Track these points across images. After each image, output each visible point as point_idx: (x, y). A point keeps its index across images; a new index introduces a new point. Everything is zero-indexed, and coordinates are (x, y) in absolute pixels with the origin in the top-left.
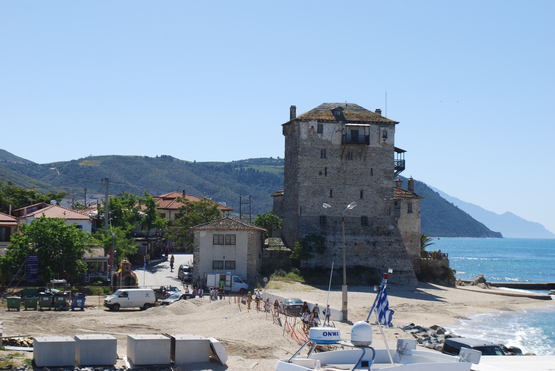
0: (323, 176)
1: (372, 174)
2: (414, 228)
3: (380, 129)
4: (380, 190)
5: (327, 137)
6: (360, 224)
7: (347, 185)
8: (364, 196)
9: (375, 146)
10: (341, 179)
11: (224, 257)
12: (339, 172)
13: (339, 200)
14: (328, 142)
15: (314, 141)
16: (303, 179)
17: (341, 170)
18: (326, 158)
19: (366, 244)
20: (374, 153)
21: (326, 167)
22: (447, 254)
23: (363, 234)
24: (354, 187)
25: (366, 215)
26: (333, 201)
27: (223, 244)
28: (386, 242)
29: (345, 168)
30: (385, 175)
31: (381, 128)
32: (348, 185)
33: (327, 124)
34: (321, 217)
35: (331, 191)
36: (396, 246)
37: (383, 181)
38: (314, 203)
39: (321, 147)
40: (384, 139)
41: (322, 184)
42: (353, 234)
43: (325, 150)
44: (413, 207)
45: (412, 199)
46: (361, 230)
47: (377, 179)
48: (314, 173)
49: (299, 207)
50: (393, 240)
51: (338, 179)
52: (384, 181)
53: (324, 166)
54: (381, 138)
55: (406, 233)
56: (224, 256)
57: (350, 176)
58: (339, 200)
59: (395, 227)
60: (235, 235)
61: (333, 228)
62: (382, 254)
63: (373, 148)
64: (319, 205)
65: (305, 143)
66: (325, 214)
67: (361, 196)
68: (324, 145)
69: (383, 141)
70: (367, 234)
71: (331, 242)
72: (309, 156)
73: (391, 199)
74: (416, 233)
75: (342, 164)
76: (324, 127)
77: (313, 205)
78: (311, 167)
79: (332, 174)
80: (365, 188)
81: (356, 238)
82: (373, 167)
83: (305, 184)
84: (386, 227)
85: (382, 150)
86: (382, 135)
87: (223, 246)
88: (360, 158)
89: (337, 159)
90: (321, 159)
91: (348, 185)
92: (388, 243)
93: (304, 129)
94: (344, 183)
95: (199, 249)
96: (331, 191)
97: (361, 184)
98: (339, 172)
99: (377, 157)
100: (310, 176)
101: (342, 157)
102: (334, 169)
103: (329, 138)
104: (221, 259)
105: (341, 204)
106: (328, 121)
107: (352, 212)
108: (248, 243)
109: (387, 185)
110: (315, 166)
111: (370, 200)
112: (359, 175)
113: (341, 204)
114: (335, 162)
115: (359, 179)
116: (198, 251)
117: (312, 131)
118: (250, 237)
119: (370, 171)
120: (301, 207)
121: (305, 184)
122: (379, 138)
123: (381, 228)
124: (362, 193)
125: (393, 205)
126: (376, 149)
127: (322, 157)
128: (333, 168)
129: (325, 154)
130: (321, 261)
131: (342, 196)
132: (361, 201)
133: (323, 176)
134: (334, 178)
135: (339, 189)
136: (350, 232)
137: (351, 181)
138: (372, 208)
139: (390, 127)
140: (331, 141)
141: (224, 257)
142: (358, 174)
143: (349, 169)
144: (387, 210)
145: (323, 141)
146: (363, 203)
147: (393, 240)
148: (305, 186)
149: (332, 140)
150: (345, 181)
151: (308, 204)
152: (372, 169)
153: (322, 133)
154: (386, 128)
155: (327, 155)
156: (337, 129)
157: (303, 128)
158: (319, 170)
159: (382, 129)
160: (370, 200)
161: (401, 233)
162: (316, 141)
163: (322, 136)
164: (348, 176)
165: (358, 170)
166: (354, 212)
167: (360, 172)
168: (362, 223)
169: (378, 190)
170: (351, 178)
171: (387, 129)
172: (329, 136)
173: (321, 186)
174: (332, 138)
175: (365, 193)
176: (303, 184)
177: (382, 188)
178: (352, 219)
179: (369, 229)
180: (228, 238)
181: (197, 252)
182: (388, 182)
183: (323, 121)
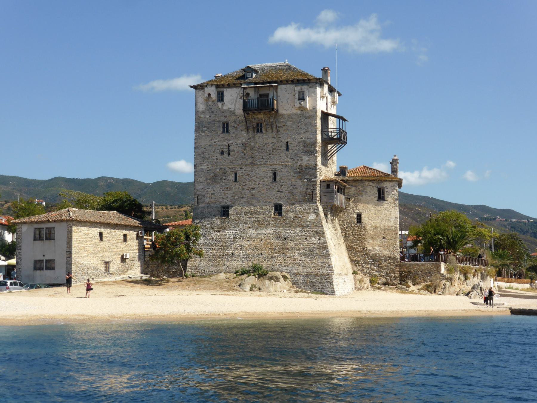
0: (226, 155)
1: (287, 148)
4: (298, 169)
5: (230, 106)
7: (255, 164)
9: (291, 112)
10: (248, 157)
11: (44, 256)
12: (245, 149)
13: (246, 185)
14: (231, 112)
15: (213, 112)
16: (201, 161)
17: (248, 147)
18: (229, 133)
20: (290, 122)
21: (229, 144)
24: (264, 167)
26: (237, 186)
27: (43, 240)
30: (305, 149)
31: (296, 88)
32: (257, 164)
33: (229, 90)
35: (236, 174)
36: (315, 240)
38: (214, 190)
39: (223, 119)
41: (224, 166)
44: (385, 193)
45: (385, 183)
47: (295, 155)
48: (214, 152)
51: (243, 158)
53: (226, 143)
55: (376, 227)
56: (107, 259)
57: (259, 153)
58: (246, 185)
59: (317, 216)
60: (54, 228)
62: (294, 251)
64: (221, 193)
65: (202, 116)
66: (229, 204)
67: (274, 179)
68: (225, 117)
69: (299, 105)
74: (392, 227)
76: (226, 93)
77: (213, 192)
78: (210, 145)
79: (236, 152)
83: (203, 167)
85: (301, 117)
87: (43, 241)
89: (243, 132)
90: (223, 135)
91: (257, 164)
92: (304, 238)
94: (252, 163)
95: (21, 246)
96: (236, 174)
99: (294, 126)
100: (209, 157)
101: (247, 129)
102: (239, 145)
103: (232, 107)
104: (41, 258)
105: (248, 189)
106: (229, 86)
107: (263, 200)
108: (67, 237)
110: (215, 144)
111: (286, 183)
112: (271, 152)
113: (248, 189)
114: (240, 137)
115: (270, 157)
116: (20, 249)
120: (198, 197)
121: (203, 167)
123: (298, 218)
124: (274, 174)
126: (293, 117)
127: (223, 132)
128: (238, 145)
130: (213, 262)
132: (274, 184)
133: (226, 155)
134: (239, 157)
135: (245, 171)
136: (256, 224)
137: (261, 160)
139: (311, 85)
140: (234, 110)
141: (44, 256)
142: (269, 151)
143: (257, 145)
144: (309, 195)
146: (276, 187)
149: (236, 109)
150: (253, 160)
151: (207, 192)
152: (287, 143)
154: (303, 87)
155: (229, 128)
157: (200, 97)
159: (298, 88)
160: (286, 183)
161: (367, 228)
162: (216, 112)
163: (222, 105)
164: (257, 154)
165: (269, 145)
167: (272, 147)
169: (296, 169)
171: (305, 88)
172: (232, 104)
173: (222, 168)
175: (278, 173)
176: (200, 167)
177: (301, 166)
180: (48, 232)
181: (20, 250)
182: (308, 158)
183: (223, 86)
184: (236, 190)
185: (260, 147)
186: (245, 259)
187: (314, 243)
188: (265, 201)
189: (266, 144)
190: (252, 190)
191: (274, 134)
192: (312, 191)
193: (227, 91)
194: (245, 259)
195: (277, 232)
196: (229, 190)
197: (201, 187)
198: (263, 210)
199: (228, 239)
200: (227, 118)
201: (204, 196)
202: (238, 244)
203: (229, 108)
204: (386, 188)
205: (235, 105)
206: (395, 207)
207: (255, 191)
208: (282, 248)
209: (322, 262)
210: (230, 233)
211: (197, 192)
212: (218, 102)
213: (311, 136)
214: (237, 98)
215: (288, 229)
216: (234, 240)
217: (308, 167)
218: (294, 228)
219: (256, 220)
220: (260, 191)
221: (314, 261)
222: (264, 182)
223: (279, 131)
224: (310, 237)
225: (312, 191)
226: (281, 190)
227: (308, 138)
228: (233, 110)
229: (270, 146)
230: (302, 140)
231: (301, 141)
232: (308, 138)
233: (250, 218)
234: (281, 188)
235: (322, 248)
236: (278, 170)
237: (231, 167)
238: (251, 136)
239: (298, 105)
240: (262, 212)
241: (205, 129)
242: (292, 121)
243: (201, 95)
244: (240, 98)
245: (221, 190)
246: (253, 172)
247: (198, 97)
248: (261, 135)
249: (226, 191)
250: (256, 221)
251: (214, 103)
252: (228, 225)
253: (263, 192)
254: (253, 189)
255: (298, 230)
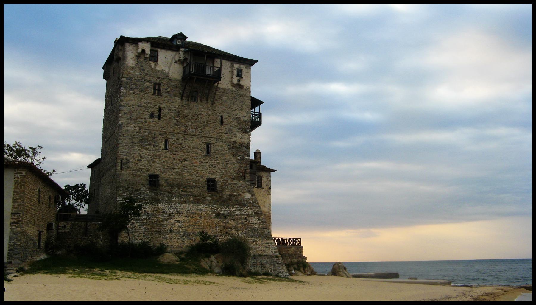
0: (156, 119)
1: (222, 122)
2: (265, 206)
3: (233, 66)
5: (163, 68)
6: (206, 188)
8: (212, 150)
12: (178, 116)
14: (164, 74)
15: (144, 70)
18: (161, 96)
19: (215, 218)
22: (301, 239)
23: (210, 203)
24: (198, 138)
25: (213, 177)
26: (168, 155)
28: (241, 214)
29: (186, 111)
32: (190, 135)
33: (163, 51)
34: (150, 176)
35: (166, 141)
36: (255, 220)
37: (236, 134)
38: (141, 157)
39: (155, 80)
40: (238, 78)
42: (197, 201)
43: (159, 85)
44: (262, 181)
45: (262, 172)
46: (208, 198)
49: (119, 161)
50: (250, 213)
52: (237, 134)
53: (158, 106)
54: (235, 77)
57: (192, 123)
58: (178, 155)
59: (252, 195)
61: (168, 193)
63: (224, 89)
65: (132, 72)
66: (158, 174)
67: (208, 152)
68: (158, 78)
70: (215, 204)
71: (164, 212)
72: (136, 90)
73: (246, 158)
74: (267, 212)
75: (182, 106)
77: (140, 158)
80: (212, 141)
81: (201, 208)
82: (224, 114)
83: (129, 128)
84: (240, 195)
86: (235, 73)
88: (207, 101)
89: (176, 98)
91: (190, 135)
93: (130, 53)
94: (185, 132)
96: (166, 141)
97: (207, 135)
98: (178, 116)
99: (229, 102)
100: (137, 118)
103: (166, 70)
108: (14, 192)
109: (242, 140)
112: (206, 123)
113: (180, 160)
115: (204, 128)
117: (143, 57)
118: (19, 180)
119: (219, 118)
120: (121, 161)
121: (129, 128)
122: (232, 77)
123: (234, 196)
124: (208, 146)
125: (248, 167)
129: (159, 90)
130: (149, 239)
131: (181, 149)
132: (207, 158)
135: (178, 139)
136: (192, 199)
137: (194, 130)
138: (222, 169)
142: (204, 122)
144: (241, 173)
145: (157, 72)
146: (210, 161)
147: (250, 213)
148: (129, 130)
149: (170, 72)
152: (222, 117)
153: (157, 61)
154: (242, 66)
155: (162, 91)
156: (177, 59)
157: (131, 52)
158: (149, 111)
159: (236, 66)
162: (148, 71)
163: (155, 65)
164: (190, 123)
165: (204, 116)
166: (198, 173)
168: (208, 189)
169: (230, 145)
170: (194, 126)
171: (243, 67)
173: (152, 133)
174: (170, 69)
177: (235, 142)
178: (194, 181)
179: (218, 196)
184: (167, 159)
185: (194, 116)
186: (186, 237)
187: (255, 223)
188: (197, 174)
189: (200, 114)
190: (184, 162)
191: (209, 105)
192: (245, 170)
193: (161, 52)
194: (186, 237)
195: (215, 209)
196: (159, 158)
197: (126, 151)
198: (196, 185)
199: (163, 214)
200: (159, 80)
201: (129, 162)
202: (175, 219)
203: (162, 70)
204: (263, 177)
205: (169, 68)
206: (269, 195)
207: (187, 163)
208: (224, 227)
209: (266, 243)
210: (163, 206)
211: (121, 156)
212: (150, 61)
213: (245, 114)
214: (172, 61)
215: (226, 207)
216: (170, 215)
217: (242, 145)
218: (233, 206)
219: (191, 194)
220: (192, 163)
221: (259, 242)
222: (197, 154)
223: (214, 103)
224: (250, 216)
225: (245, 170)
226: (215, 164)
227: (242, 116)
228: (167, 72)
229: (205, 118)
230: (237, 116)
231: (236, 118)
232: (242, 116)
233: (185, 191)
234: (214, 163)
235: (264, 229)
236: (212, 143)
237: (161, 133)
238: (184, 103)
239: (235, 82)
240: (196, 186)
241: (134, 86)
242: (227, 97)
243: (131, 49)
244: (175, 62)
245: (150, 157)
246: (186, 142)
247: (128, 51)
248: (195, 104)
249: (155, 158)
250: (191, 196)
251: (146, 61)
252: (160, 197)
253: (196, 165)
254: (185, 160)
255: (236, 208)
